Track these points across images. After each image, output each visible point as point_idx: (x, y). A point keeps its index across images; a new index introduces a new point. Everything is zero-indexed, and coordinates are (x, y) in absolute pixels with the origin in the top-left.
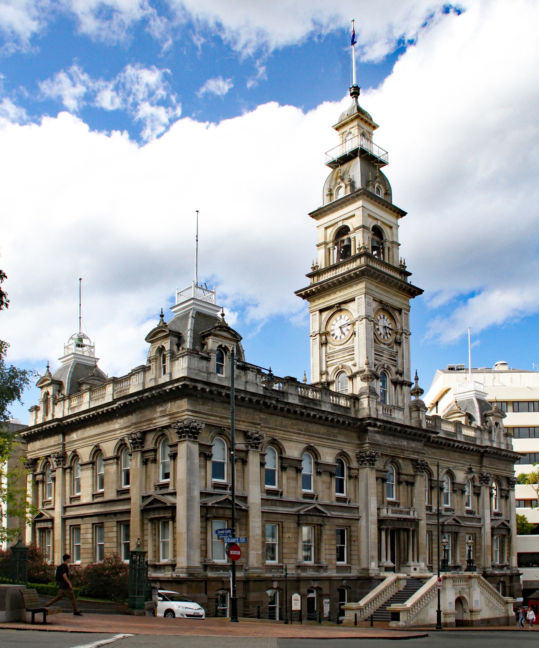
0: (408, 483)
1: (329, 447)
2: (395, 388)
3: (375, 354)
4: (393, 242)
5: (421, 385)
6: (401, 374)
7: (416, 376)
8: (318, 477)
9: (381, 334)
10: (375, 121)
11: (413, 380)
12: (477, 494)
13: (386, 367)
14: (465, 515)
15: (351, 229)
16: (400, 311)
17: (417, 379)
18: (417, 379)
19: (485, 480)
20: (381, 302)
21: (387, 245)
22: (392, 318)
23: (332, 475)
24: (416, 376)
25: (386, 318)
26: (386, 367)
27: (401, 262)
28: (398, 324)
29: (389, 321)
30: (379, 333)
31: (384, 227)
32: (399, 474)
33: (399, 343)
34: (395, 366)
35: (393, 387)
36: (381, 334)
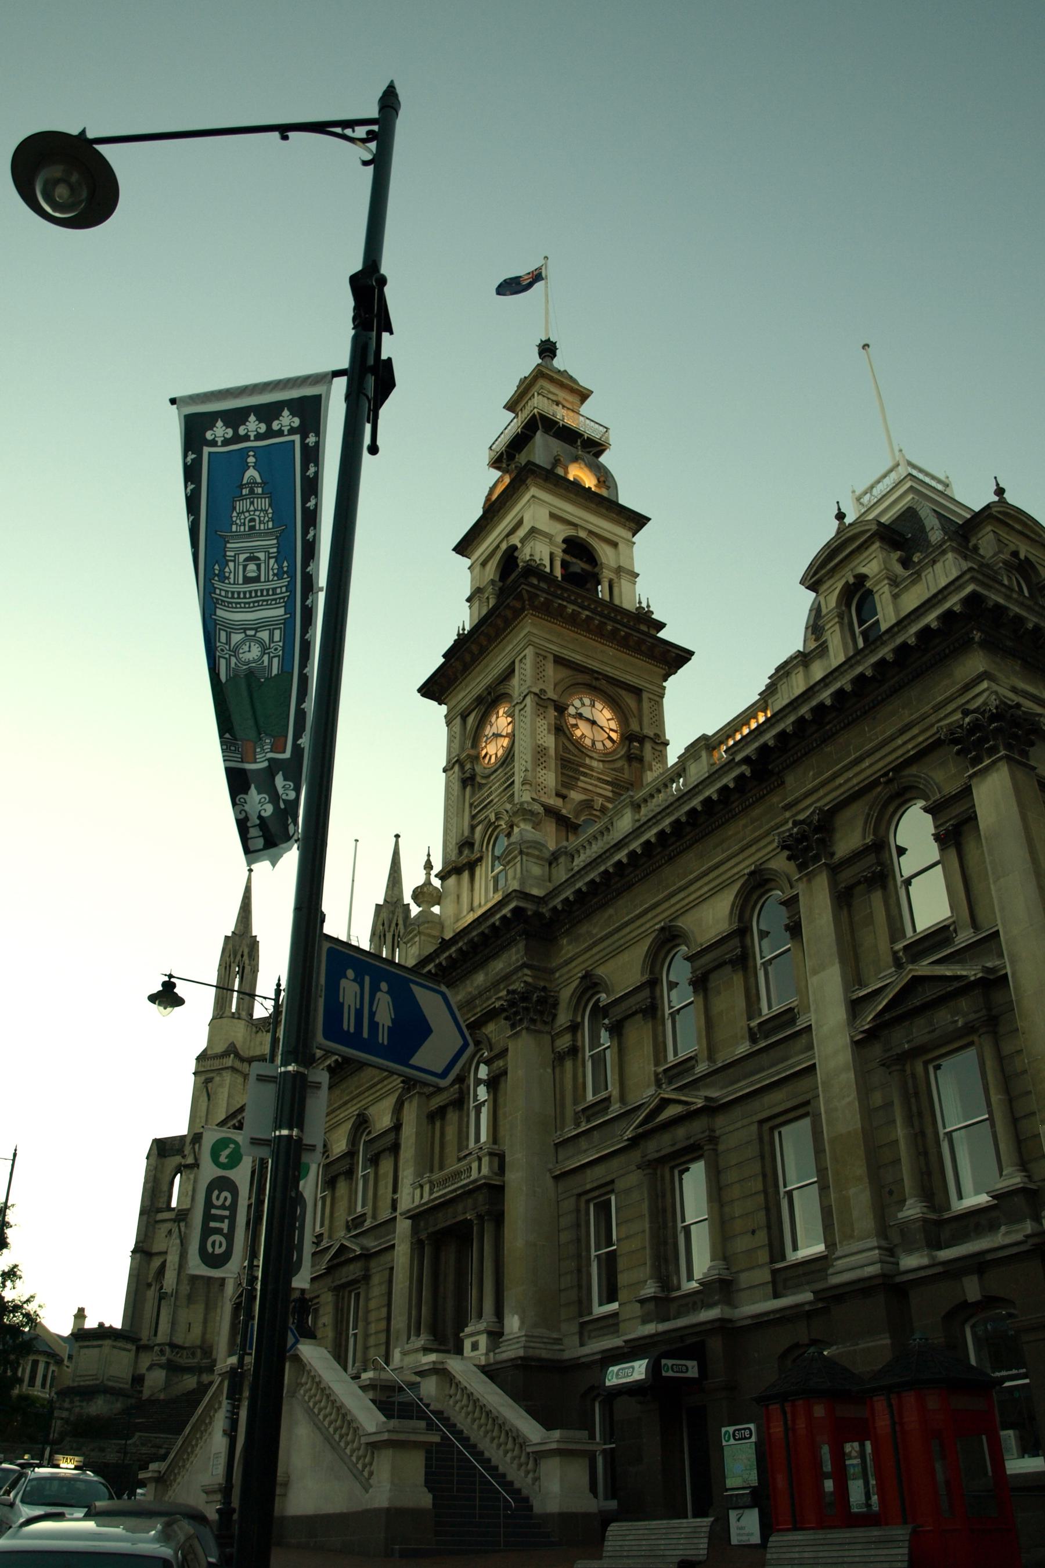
4: (619, 570)
10: (584, 382)
15: (519, 545)
21: (606, 574)
27: (640, 603)
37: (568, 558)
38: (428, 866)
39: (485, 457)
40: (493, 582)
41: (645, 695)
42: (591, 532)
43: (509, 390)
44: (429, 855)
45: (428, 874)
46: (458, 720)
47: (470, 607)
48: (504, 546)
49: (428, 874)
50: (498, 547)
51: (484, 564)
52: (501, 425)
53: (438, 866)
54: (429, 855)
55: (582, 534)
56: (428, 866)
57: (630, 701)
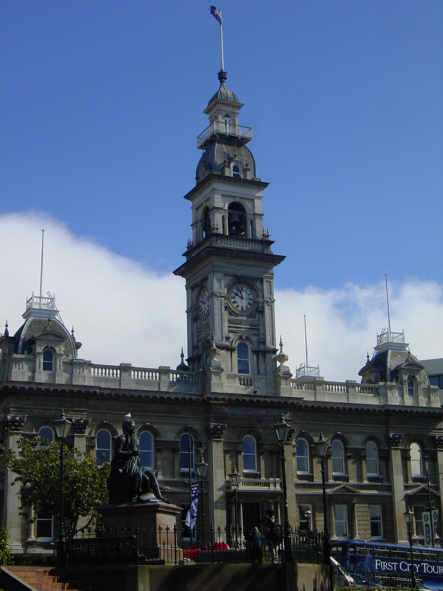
0: (272, 453)
1: (171, 424)
2: (258, 357)
3: (229, 327)
5: (285, 352)
6: (264, 343)
7: (281, 342)
8: (158, 454)
9: (238, 306)
11: (278, 347)
12: (385, 458)
13: (244, 337)
14: (366, 482)
16: (261, 280)
17: (281, 345)
18: (281, 345)
19: (393, 442)
20: (235, 276)
21: (249, 217)
22: (252, 288)
23: (175, 451)
24: (281, 342)
25: (244, 289)
26: (244, 337)
28: (260, 293)
29: (249, 292)
30: (235, 305)
31: (242, 202)
32: (259, 445)
33: (262, 312)
34: (258, 335)
35: (255, 357)
36: (238, 306)
37: (232, 212)
38: (182, 356)
39: (195, 143)
40: (201, 221)
41: (265, 280)
42: (241, 198)
43: (205, 106)
44: (182, 351)
45: (182, 359)
46: (190, 290)
47: (193, 229)
48: (204, 205)
49: (182, 359)
50: (202, 204)
51: (197, 209)
52: (201, 126)
53: (186, 357)
54: (182, 351)
55: (237, 200)
56: (182, 356)
57: (258, 284)
